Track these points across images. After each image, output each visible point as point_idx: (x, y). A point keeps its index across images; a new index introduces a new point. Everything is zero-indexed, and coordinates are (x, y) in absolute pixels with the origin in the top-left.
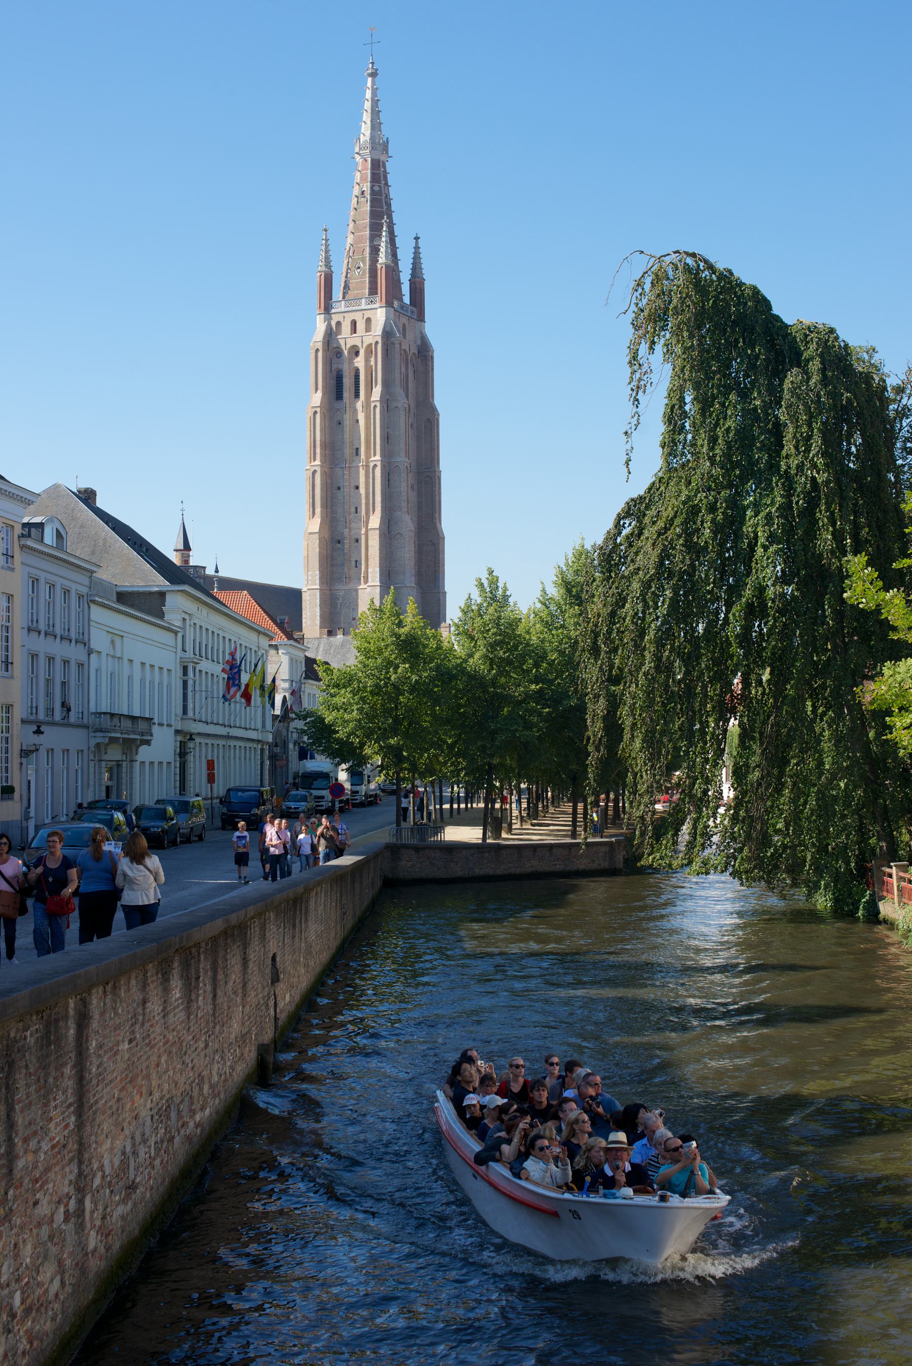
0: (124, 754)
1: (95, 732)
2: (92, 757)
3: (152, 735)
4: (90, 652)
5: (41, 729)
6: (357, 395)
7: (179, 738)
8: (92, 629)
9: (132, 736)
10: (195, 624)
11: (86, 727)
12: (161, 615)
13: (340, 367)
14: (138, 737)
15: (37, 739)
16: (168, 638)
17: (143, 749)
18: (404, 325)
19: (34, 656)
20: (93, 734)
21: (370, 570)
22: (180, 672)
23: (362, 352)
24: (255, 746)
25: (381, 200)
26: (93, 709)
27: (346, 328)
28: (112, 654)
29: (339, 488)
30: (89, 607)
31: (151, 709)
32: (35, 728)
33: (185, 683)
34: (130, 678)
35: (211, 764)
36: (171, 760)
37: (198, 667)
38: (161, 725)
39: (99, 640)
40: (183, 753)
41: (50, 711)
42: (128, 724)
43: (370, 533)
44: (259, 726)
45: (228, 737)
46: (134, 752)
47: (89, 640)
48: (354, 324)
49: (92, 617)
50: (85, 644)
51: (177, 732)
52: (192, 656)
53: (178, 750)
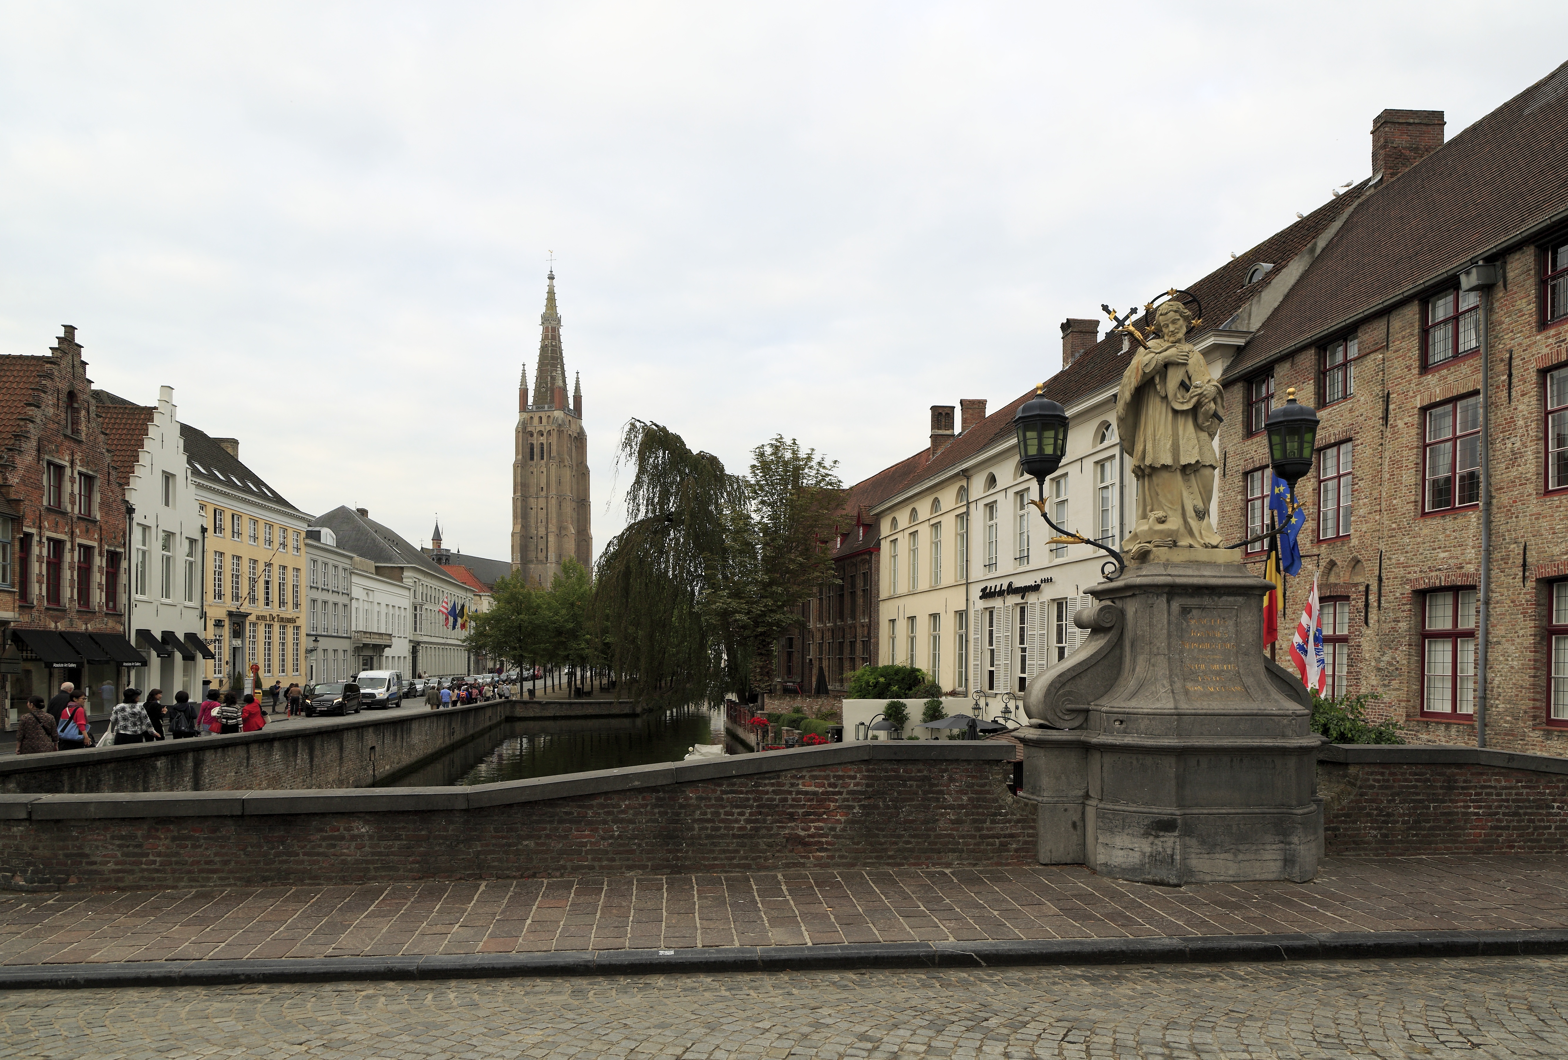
4: (352, 599)
6: (542, 458)
12: (401, 580)
16: (406, 593)
23: (545, 434)
37: (424, 607)
39: (356, 592)
48: (541, 418)
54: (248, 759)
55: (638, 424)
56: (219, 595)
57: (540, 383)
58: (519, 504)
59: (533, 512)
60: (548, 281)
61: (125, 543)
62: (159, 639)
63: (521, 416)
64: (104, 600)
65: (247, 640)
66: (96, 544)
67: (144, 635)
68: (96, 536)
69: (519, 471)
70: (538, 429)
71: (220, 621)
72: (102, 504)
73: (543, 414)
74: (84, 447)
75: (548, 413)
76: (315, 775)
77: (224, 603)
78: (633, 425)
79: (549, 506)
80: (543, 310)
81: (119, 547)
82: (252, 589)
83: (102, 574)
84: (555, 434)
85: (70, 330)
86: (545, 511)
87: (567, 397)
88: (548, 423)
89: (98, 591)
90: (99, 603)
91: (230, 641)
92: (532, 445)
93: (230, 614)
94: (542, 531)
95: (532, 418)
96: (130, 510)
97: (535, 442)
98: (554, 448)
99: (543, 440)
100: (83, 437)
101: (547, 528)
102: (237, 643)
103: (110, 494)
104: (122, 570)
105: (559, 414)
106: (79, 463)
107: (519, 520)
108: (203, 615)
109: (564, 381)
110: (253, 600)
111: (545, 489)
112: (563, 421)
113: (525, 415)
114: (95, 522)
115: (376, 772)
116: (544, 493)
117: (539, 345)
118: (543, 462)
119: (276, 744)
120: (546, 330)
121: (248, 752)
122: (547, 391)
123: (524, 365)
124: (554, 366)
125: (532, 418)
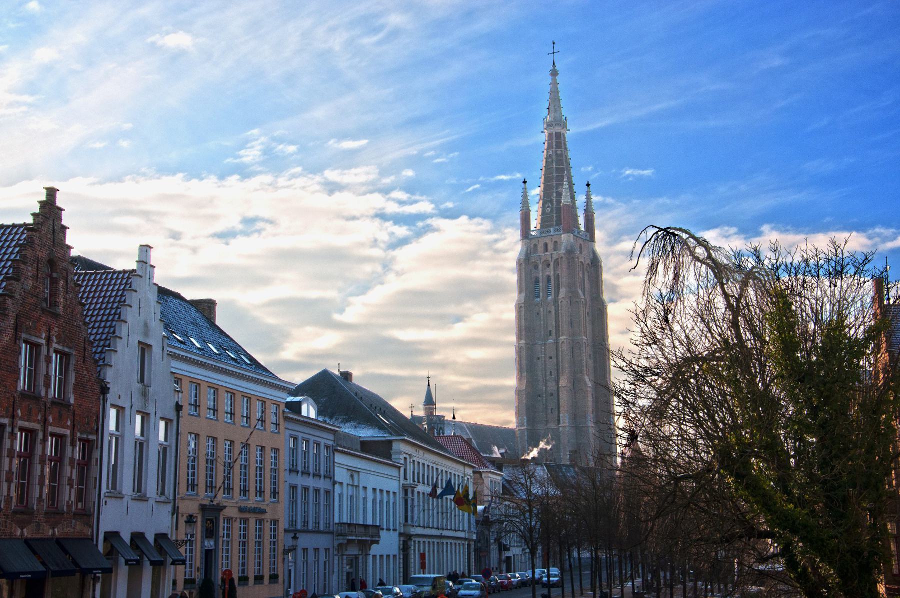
0: (360, 550)
1: (338, 536)
2: (335, 553)
3: (379, 537)
4: (334, 483)
5: (298, 535)
7: (402, 539)
8: (336, 468)
9: (364, 538)
10: (414, 461)
11: (332, 533)
12: (389, 457)
13: (537, 275)
14: (369, 539)
15: (294, 543)
16: (393, 472)
17: (374, 546)
18: (580, 244)
19: (293, 488)
20: (337, 538)
21: (561, 415)
22: (402, 495)
23: (552, 264)
24: (463, 542)
25: (563, 159)
26: (336, 520)
27: (540, 248)
28: (351, 483)
29: (539, 359)
30: (334, 454)
31: (381, 519)
32: (292, 535)
33: (406, 501)
34: (365, 499)
35: (423, 556)
36: (396, 552)
37: (416, 490)
38: (388, 530)
39: (341, 475)
40: (405, 548)
41: (306, 523)
42: (362, 530)
43: (560, 390)
44: (466, 528)
45: (441, 537)
46: (368, 549)
47: (334, 476)
48: (546, 245)
49: (336, 461)
50: (331, 478)
51: (400, 534)
52: (412, 482)
53: (401, 547)
56: (192, 486)
58: (524, 353)
60: (549, 80)
61: (97, 429)
64: (73, 499)
65: (221, 540)
66: (68, 432)
67: (112, 536)
68: (69, 423)
69: (523, 313)
71: (191, 516)
74: (61, 321)
77: (197, 495)
81: (92, 434)
82: (227, 477)
83: (73, 467)
84: (564, 264)
85: (52, 193)
86: (554, 360)
87: (575, 218)
89: (68, 487)
90: (68, 502)
91: (202, 542)
93: (203, 508)
95: (535, 245)
96: (105, 390)
98: (564, 280)
99: (550, 272)
101: (557, 382)
102: (209, 544)
103: (85, 372)
104: (93, 461)
105: (565, 239)
106: (55, 340)
107: (525, 374)
108: (175, 511)
110: (229, 489)
114: (68, 405)
122: (551, 212)
124: (560, 180)
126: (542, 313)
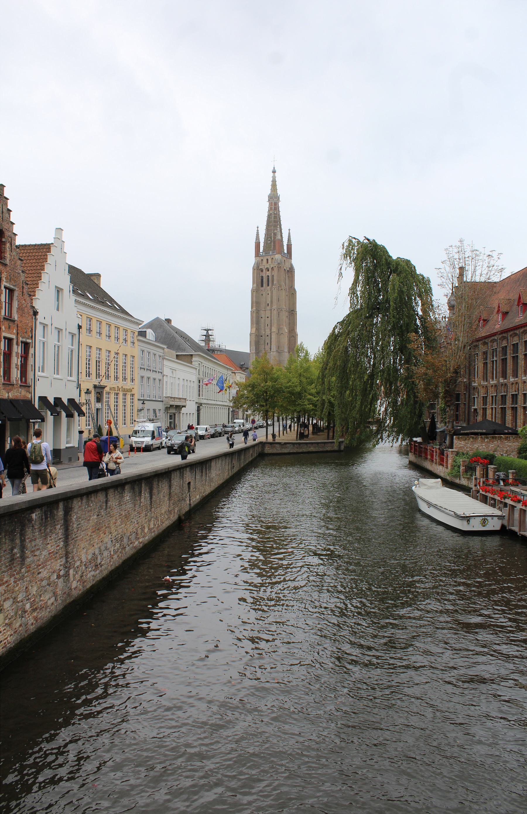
6: (268, 285)
23: (270, 270)
48: (267, 260)
54: (107, 502)
55: (354, 240)
57: (267, 238)
58: (254, 315)
59: (262, 320)
61: (32, 336)
62: (53, 403)
63: (256, 259)
64: (19, 376)
67: (43, 400)
68: (15, 331)
70: (266, 267)
72: (18, 309)
73: (269, 258)
74: (8, 269)
75: (272, 257)
76: (153, 509)
77: (91, 379)
78: (350, 241)
79: (272, 315)
80: (269, 192)
81: (28, 339)
83: (18, 358)
84: (276, 269)
86: (269, 318)
87: (282, 246)
88: (272, 263)
89: (16, 369)
90: (16, 378)
91: (95, 405)
92: (262, 277)
93: (95, 387)
94: (268, 332)
95: (262, 260)
96: (35, 313)
97: (264, 275)
98: (275, 278)
99: (269, 273)
100: (8, 262)
101: (271, 330)
103: (24, 302)
104: (30, 355)
105: (278, 257)
106: (5, 280)
108: (79, 386)
109: (281, 236)
111: (270, 305)
112: (281, 261)
113: (258, 258)
114: (14, 321)
115: (191, 501)
116: (269, 308)
117: (267, 214)
118: (269, 288)
119: (127, 487)
120: (271, 204)
121: (107, 496)
123: (258, 227)
124: (276, 226)
125: (262, 260)
126: (264, 295)
